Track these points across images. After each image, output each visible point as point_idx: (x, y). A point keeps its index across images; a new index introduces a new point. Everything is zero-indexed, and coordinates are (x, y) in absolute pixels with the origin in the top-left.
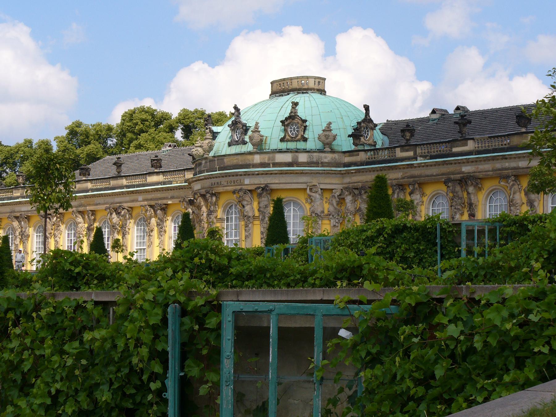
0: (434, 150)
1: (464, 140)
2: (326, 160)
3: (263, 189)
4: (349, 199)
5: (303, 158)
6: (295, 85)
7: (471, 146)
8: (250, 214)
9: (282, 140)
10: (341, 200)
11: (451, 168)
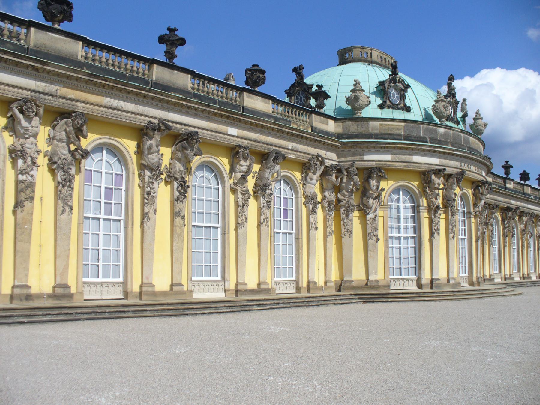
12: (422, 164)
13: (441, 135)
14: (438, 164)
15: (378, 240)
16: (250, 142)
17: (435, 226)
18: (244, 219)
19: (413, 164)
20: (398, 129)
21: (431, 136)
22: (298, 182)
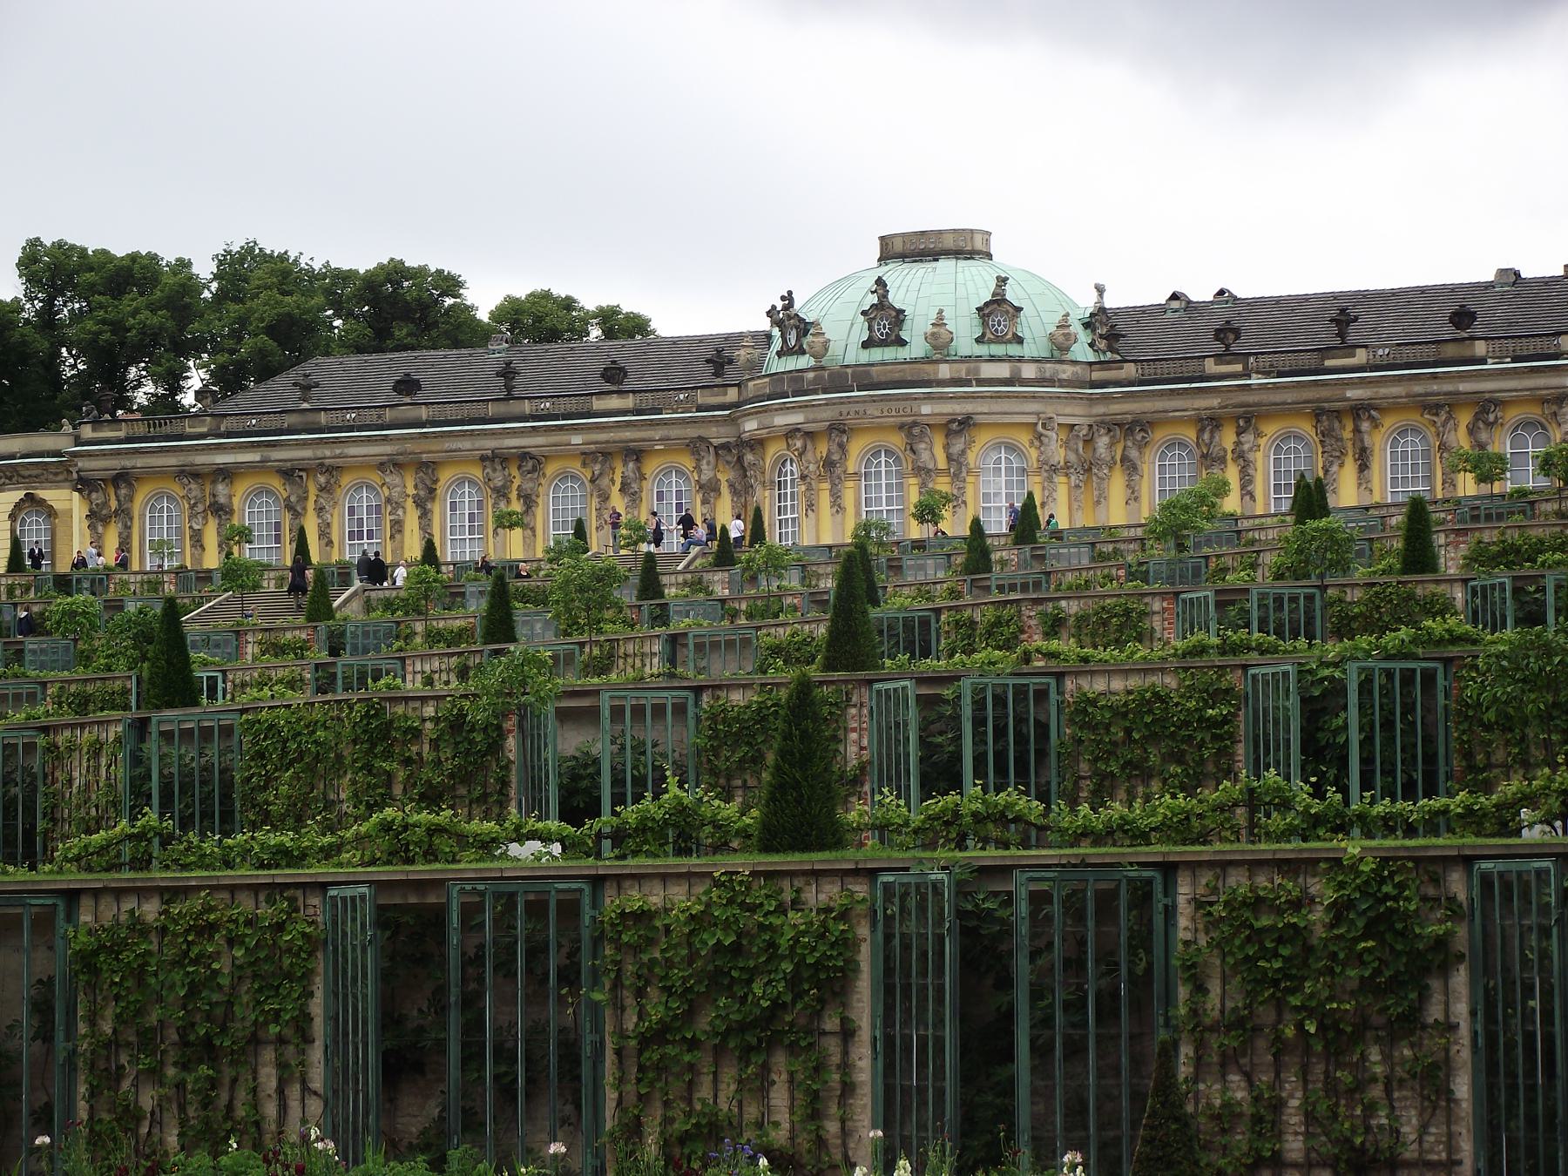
0: (1284, 362)
1: (1351, 349)
2: (1064, 376)
3: (960, 423)
4: (1103, 442)
5: (1029, 371)
6: (949, 243)
7: (1361, 357)
8: (931, 466)
9: (979, 341)
10: (1089, 441)
11: (1324, 393)
13: (809, 383)
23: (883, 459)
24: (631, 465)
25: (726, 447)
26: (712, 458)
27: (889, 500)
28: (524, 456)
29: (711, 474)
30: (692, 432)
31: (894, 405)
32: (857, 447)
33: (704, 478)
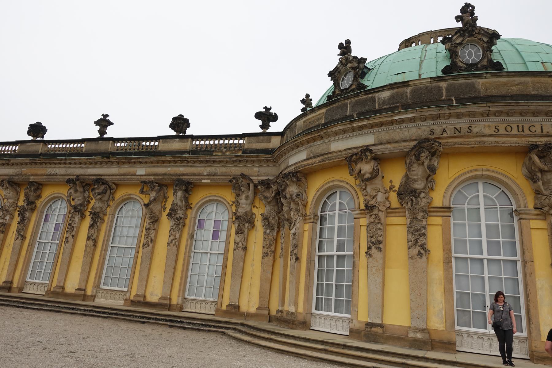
12: (341, 151)
13: (384, 102)
14: (373, 143)
15: (297, 259)
16: (157, 177)
17: (372, 237)
18: (150, 241)
19: (329, 156)
20: (319, 119)
21: (363, 110)
22: (228, 203)
23: (481, 193)
24: (180, 194)
25: (267, 184)
26: (251, 193)
27: (493, 247)
28: (99, 181)
29: (248, 209)
30: (235, 170)
31: (516, 121)
32: (449, 173)
33: (241, 211)
